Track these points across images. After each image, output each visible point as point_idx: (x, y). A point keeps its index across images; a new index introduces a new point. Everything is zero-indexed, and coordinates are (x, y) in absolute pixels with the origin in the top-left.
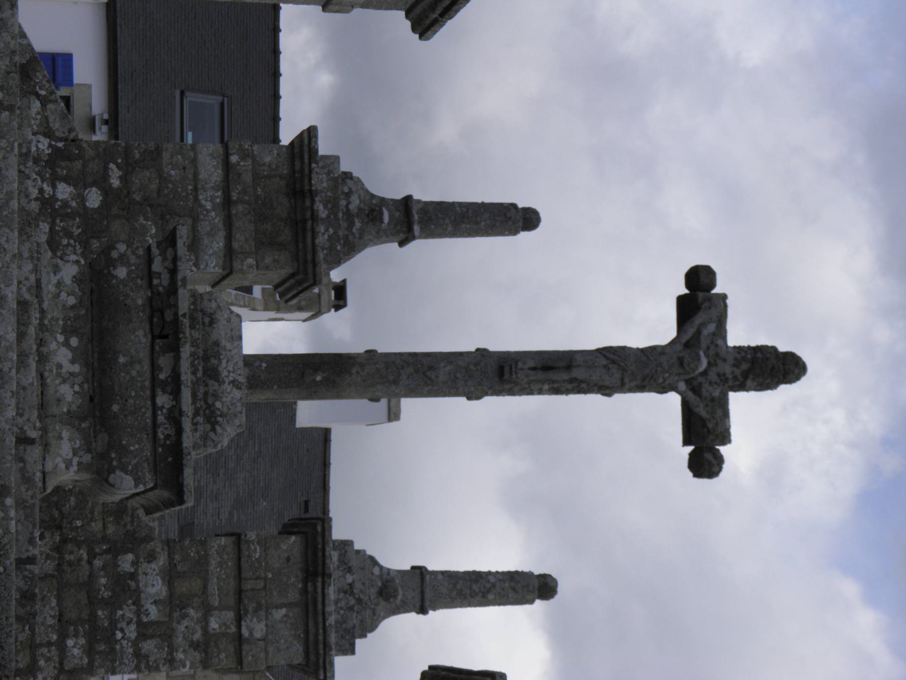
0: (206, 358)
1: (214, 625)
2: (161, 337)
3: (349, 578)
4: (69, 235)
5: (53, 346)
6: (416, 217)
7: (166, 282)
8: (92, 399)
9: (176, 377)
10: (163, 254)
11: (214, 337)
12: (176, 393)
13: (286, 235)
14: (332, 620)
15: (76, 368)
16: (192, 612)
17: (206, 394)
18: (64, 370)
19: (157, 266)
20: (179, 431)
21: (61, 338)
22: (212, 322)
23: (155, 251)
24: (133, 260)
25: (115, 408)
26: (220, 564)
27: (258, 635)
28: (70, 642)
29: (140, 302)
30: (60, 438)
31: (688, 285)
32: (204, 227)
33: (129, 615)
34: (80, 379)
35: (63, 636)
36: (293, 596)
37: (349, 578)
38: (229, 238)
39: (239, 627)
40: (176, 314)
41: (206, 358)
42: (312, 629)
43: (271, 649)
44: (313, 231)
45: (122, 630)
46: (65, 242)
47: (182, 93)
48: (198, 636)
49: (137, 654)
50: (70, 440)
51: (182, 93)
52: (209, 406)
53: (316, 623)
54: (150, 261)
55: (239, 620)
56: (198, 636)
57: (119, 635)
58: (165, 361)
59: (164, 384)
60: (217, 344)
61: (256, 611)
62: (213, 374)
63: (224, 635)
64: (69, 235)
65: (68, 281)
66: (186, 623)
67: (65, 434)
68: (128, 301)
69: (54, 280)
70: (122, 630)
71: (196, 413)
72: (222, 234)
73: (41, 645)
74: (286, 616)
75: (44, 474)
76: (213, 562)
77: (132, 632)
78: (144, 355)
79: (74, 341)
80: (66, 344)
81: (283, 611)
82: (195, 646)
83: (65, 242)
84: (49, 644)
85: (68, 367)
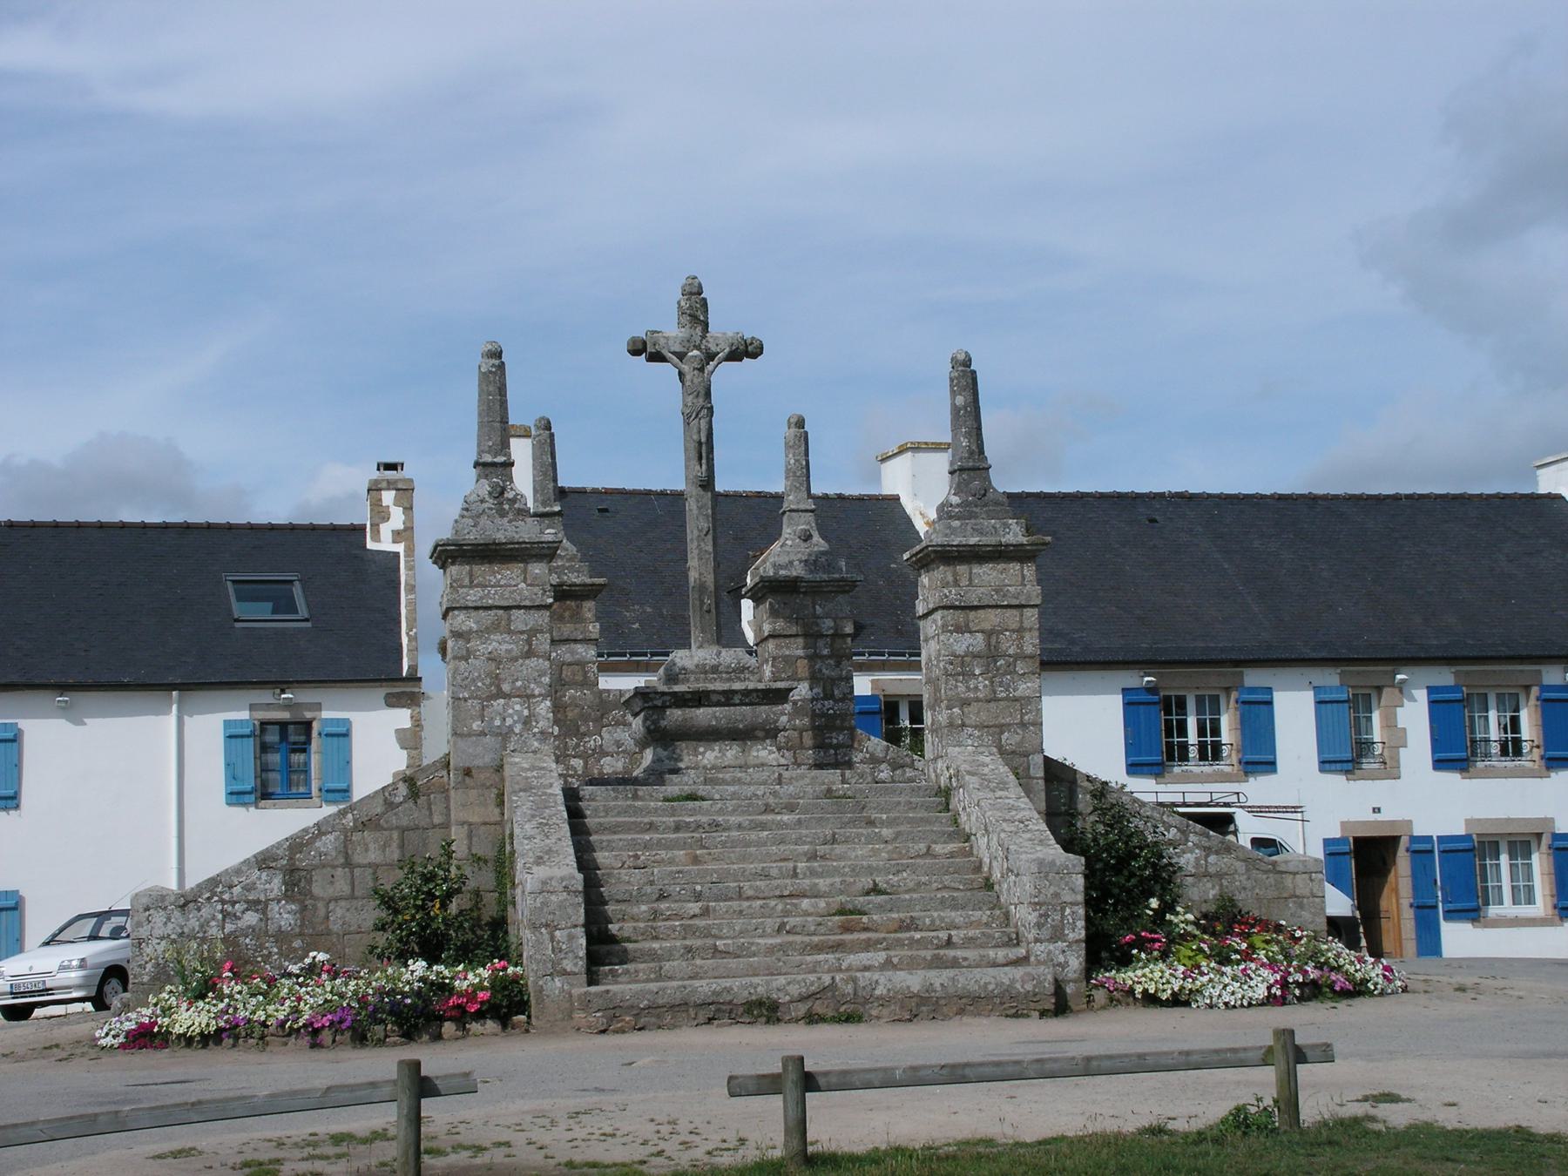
0: (706, 672)
1: (825, 652)
2: (700, 701)
3: (796, 563)
4: (578, 745)
5: (706, 761)
6: (548, 509)
7: (668, 698)
8: (734, 740)
9: (724, 692)
10: (652, 700)
11: (693, 668)
12: (735, 692)
13: (571, 603)
14: (825, 577)
15: (717, 748)
16: (817, 667)
17: (727, 673)
18: (719, 755)
19: (659, 703)
20: (756, 690)
21: (700, 757)
22: (684, 669)
23: (650, 704)
24: (655, 717)
25: (741, 726)
26: (788, 648)
27: (832, 624)
28: (835, 741)
29: (680, 713)
30: (757, 757)
31: (640, 355)
32: (568, 658)
33: (819, 706)
34: (724, 747)
35: (831, 746)
36: (808, 601)
37: (796, 563)
38: (575, 641)
39: (827, 636)
40: (688, 692)
41: (706, 672)
42: (830, 588)
43: (840, 616)
44: (570, 586)
45: (828, 710)
46: (582, 748)
47: (237, 620)
48: (832, 662)
49: (842, 700)
50: (758, 751)
51: (237, 620)
52: (734, 671)
53: (827, 586)
54: (656, 707)
55: (823, 636)
56: (832, 662)
57: (831, 712)
58: (714, 698)
59: (728, 699)
60: (697, 666)
61: (817, 625)
62: (715, 669)
63: (831, 645)
64: (578, 745)
65: (666, 753)
66: (824, 671)
67: (755, 754)
68: (680, 719)
69: (667, 761)
70: (828, 710)
71: (739, 679)
72: (573, 646)
73: (837, 759)
74: (820, 606)
75: (779, 766)
76: (787, 653)
77: (829, 704)
78: (710, 710)
79: (701, 750)
80: (703, 754)
81: (817, 607)
82: (838, 664)
83: (582, 748)
84: (836, 754)
85: (716, 753)
